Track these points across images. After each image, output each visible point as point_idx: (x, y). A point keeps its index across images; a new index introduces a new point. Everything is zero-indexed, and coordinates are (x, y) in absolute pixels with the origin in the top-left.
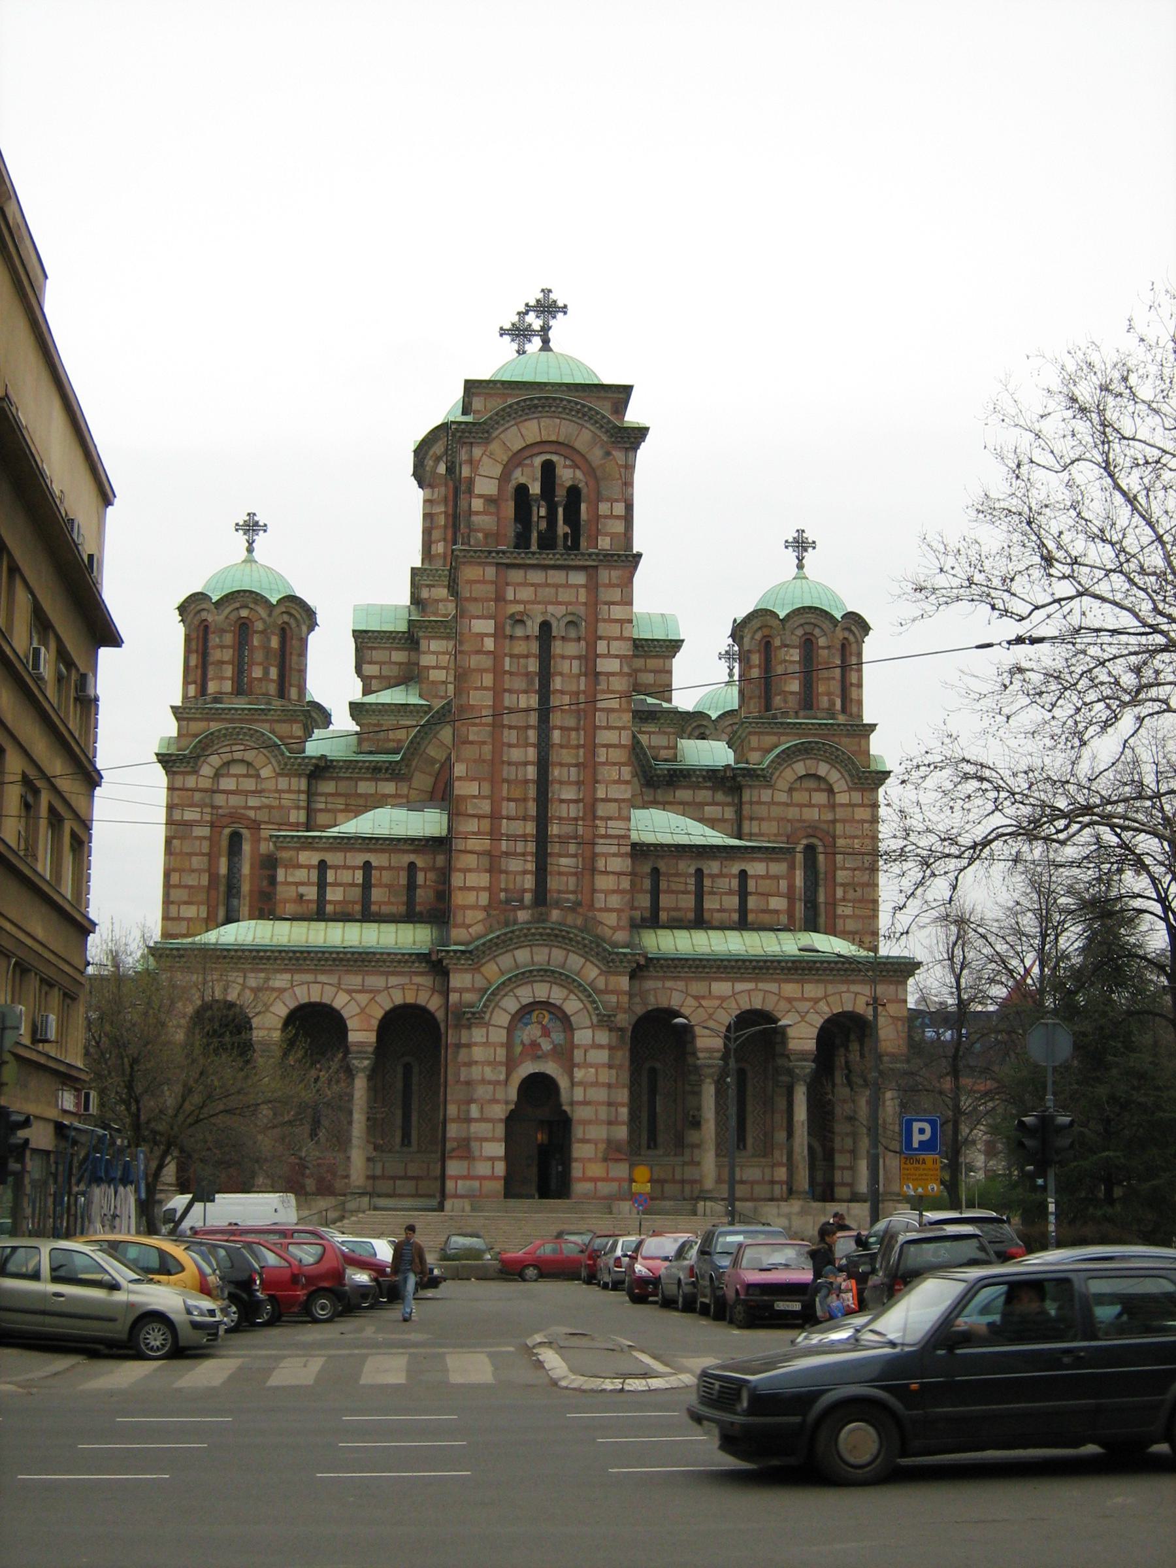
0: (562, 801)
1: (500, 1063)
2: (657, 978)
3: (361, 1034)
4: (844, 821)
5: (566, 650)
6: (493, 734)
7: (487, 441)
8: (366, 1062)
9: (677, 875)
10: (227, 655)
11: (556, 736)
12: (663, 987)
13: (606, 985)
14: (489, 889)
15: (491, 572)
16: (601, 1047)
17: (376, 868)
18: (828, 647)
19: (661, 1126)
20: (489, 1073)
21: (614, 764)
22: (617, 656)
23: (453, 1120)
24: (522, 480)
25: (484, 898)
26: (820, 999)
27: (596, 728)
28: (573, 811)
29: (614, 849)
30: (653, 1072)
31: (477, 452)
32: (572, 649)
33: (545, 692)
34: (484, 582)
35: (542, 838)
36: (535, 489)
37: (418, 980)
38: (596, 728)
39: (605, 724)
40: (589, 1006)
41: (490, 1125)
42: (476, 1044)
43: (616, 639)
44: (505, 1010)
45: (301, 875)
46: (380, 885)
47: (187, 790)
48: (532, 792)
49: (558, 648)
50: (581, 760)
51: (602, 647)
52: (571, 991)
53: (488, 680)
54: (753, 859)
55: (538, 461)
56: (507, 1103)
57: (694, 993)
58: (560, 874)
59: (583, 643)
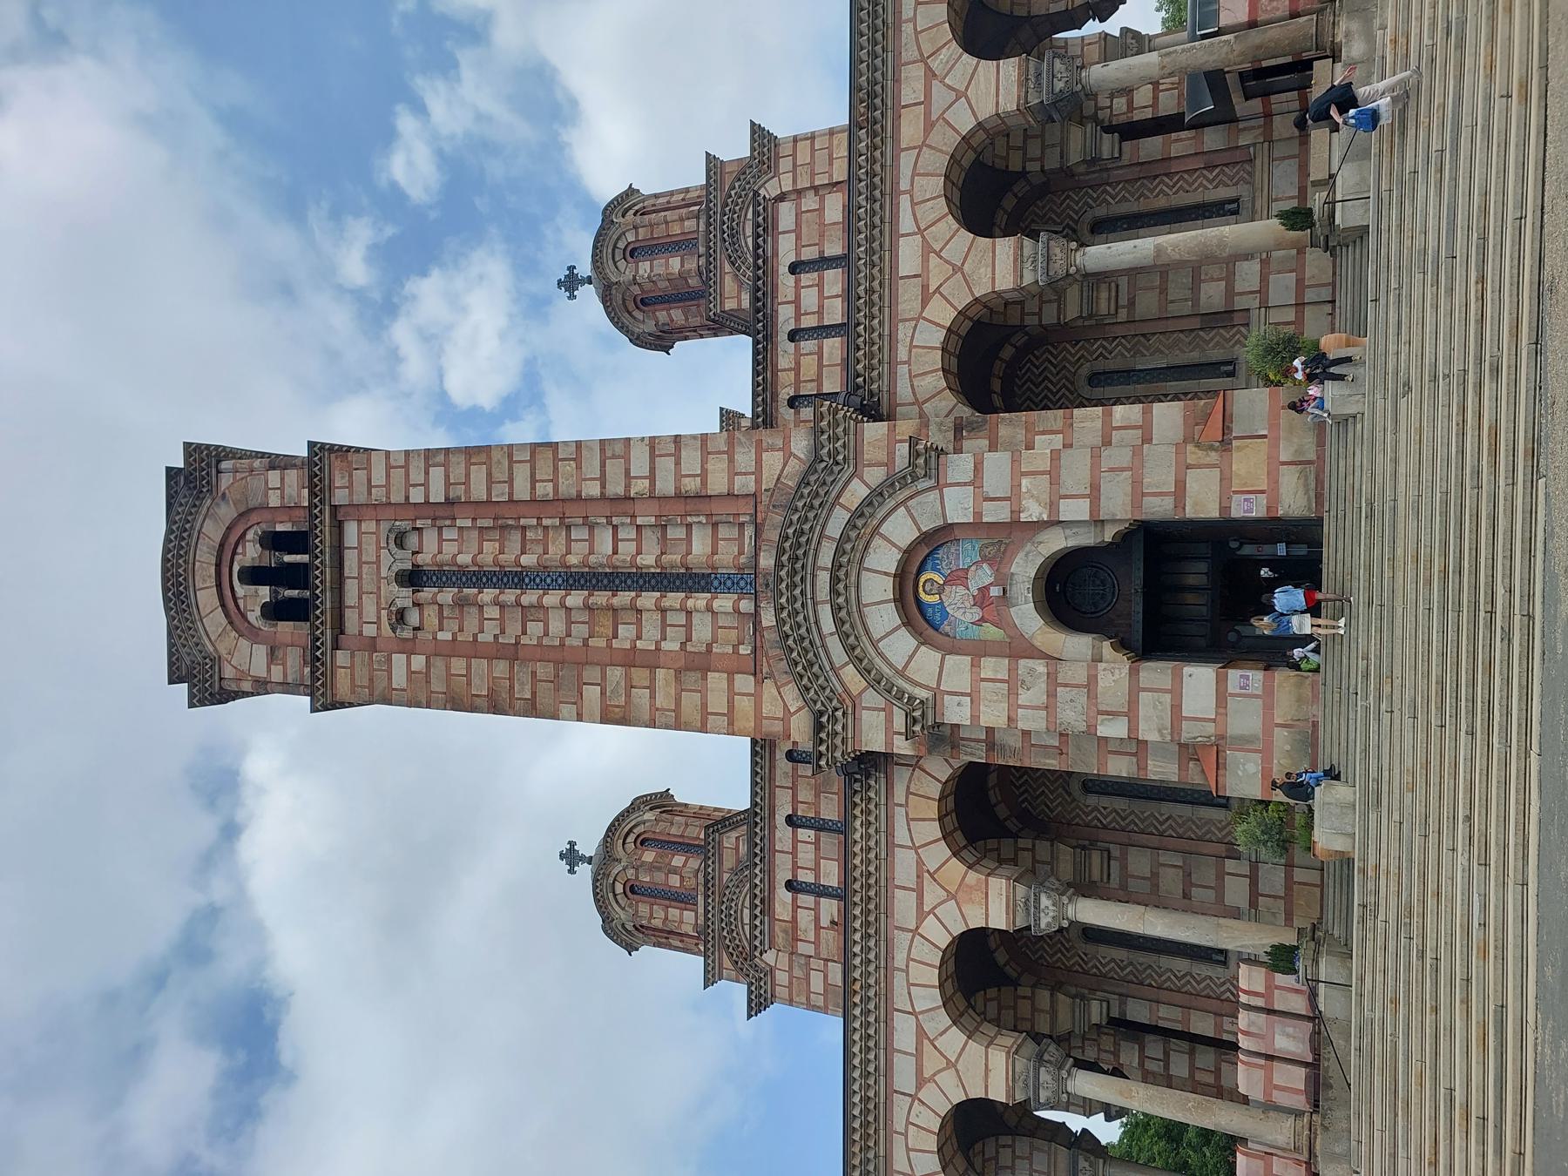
0: (615, 552)
1: (1012, 670)
2: (892, 374)
3: (994, 903)
4: (813, 175)
5: (432, 549)
6: (524, 661)
7: (216, 661)
8: (1045, 901)
9: (797, 369)
10: (659, 913)
11: (528, 560)
12: (908, 362)
13: (879, 465)
14: (731, 674)
15: (342, 657)
16: (978, 468)
17: (795, 809)
18: (635, 228)
19: (1194, 356)
20: (1033, 694)
21: (556, 469)
22: (427, 473)
23: (1142, 766)
24: (258, 610)
25: (745, 683)
26: (928, 68)
27: (511, 501)
28: (627, 533)
29: (669, 463)
30: (1095, 379)
31: (228, 672)
32: (430, 538)
33: (480, 578)
34: (352, 667)
35: (662, 581)
36: (265, 592)
37: (899, 794)
38: (511, 501)
39: (506, 488)
40: (901, 496)
42: (975, 717)
43: (407, 475)
44: (911, 657)
45: (805, 918)
46: (817, 805)
47: (791, 983)
48: (601, 598)
49: (424, 559)
50: (557, 522)
51: (417, 496)
52: (875, 531)
53: (458, 665)
54: (775, 254)
55: (240, 590)
56: (1097, 659)
57: (917, 304)
58: (715, 552)
59: (419, 524)
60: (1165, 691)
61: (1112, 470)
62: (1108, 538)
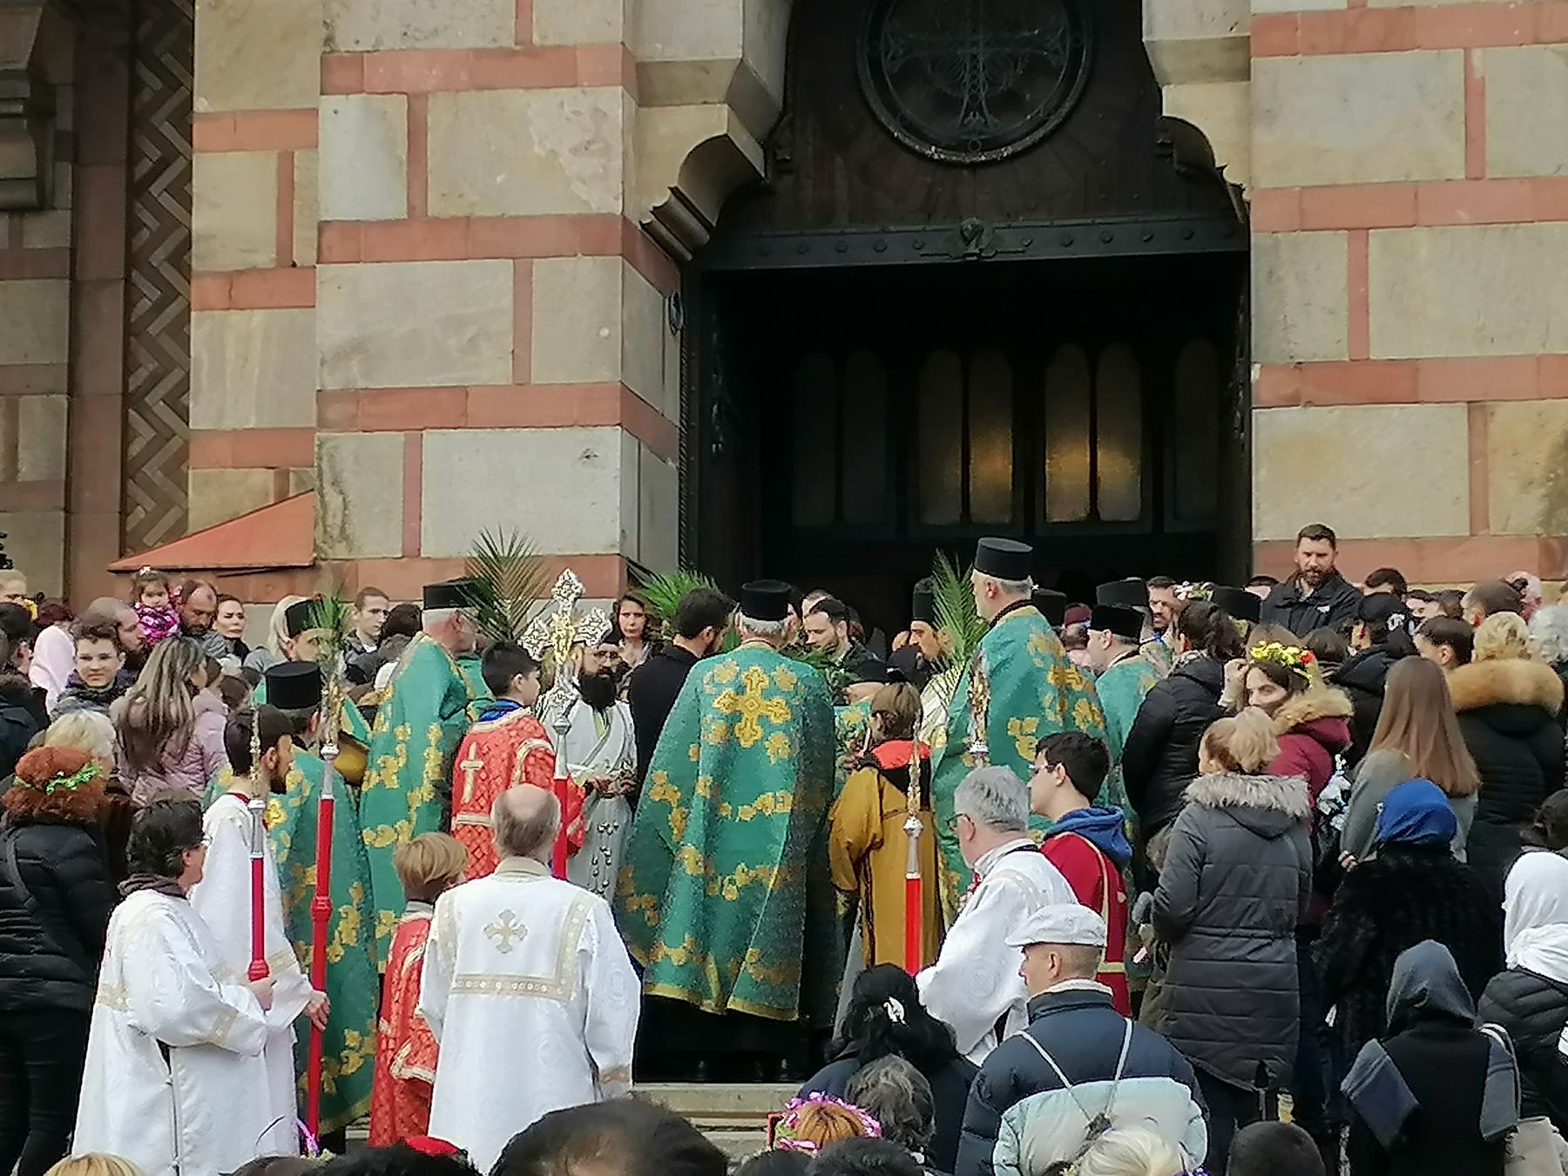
23: (239, 288)
41: (492, 280)
56: (647, 84)
60: (520, 356)
61: (1474, 91)
62: (1177, 101)
